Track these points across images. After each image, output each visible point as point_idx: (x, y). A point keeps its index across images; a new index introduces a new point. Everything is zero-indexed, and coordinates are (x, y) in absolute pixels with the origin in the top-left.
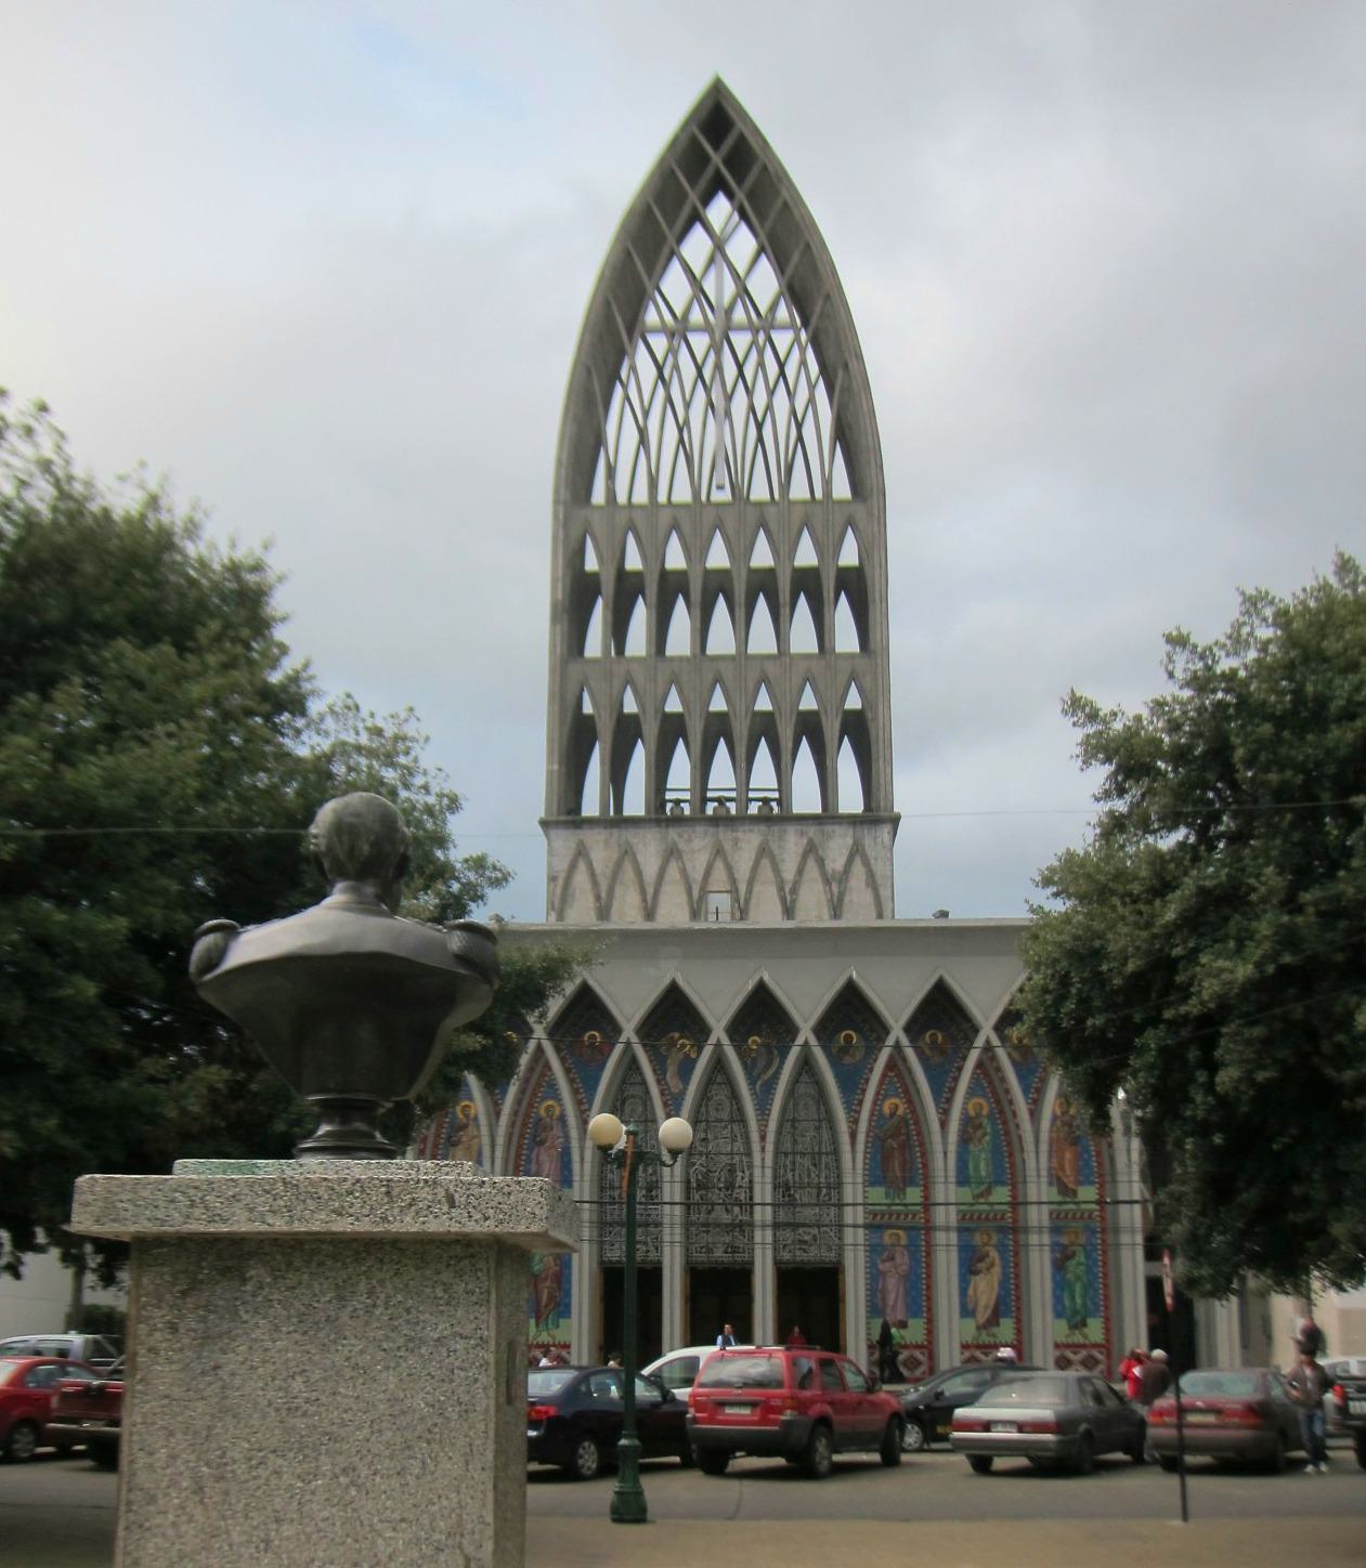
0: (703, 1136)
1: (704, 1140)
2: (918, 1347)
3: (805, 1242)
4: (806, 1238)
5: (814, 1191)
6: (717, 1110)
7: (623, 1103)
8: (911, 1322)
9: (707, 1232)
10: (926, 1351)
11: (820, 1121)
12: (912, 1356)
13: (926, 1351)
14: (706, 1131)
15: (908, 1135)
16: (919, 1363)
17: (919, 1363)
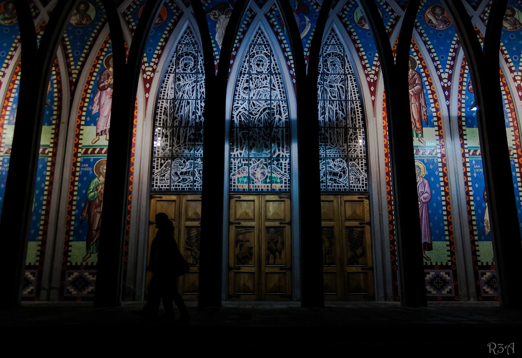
0: (246, 85)
1: (246, 88)
2: (442, 267)
3: (335, 174)
4: (337, 170)
5: (342, 131)
6: (258, 65)
7: (178, 59)
8: (435, 243)
9: (249, 165)
10: (451, 271)
11: (345, 75)
12: (438, 276)
13: (451, 271)
14: (247, 81)
15: (422, 84)
16: (445, 283)
17: (445, 283)
